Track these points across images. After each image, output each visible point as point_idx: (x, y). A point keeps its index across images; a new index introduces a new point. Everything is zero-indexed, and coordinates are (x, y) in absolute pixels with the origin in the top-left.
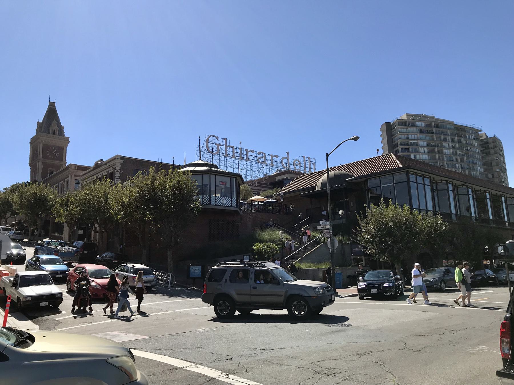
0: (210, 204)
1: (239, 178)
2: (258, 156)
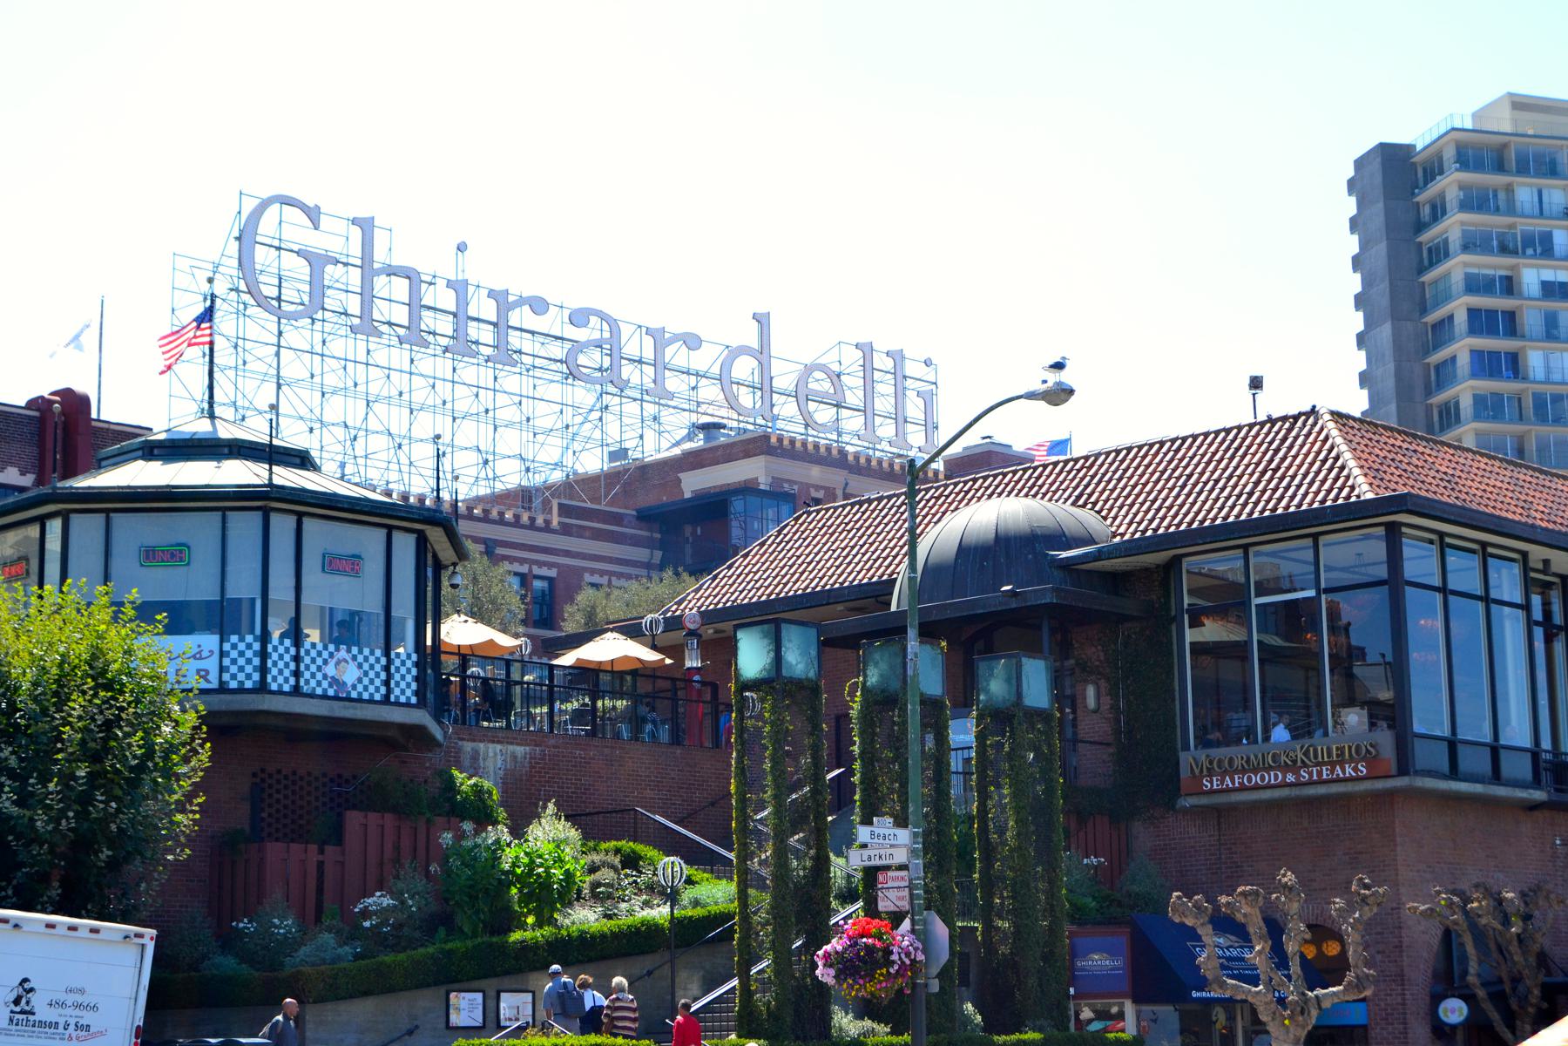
0: (262, 687)
1: (436, 535)
2: (572, 332)
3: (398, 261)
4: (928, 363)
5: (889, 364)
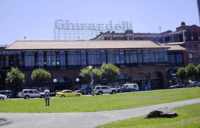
5: (126, 23)
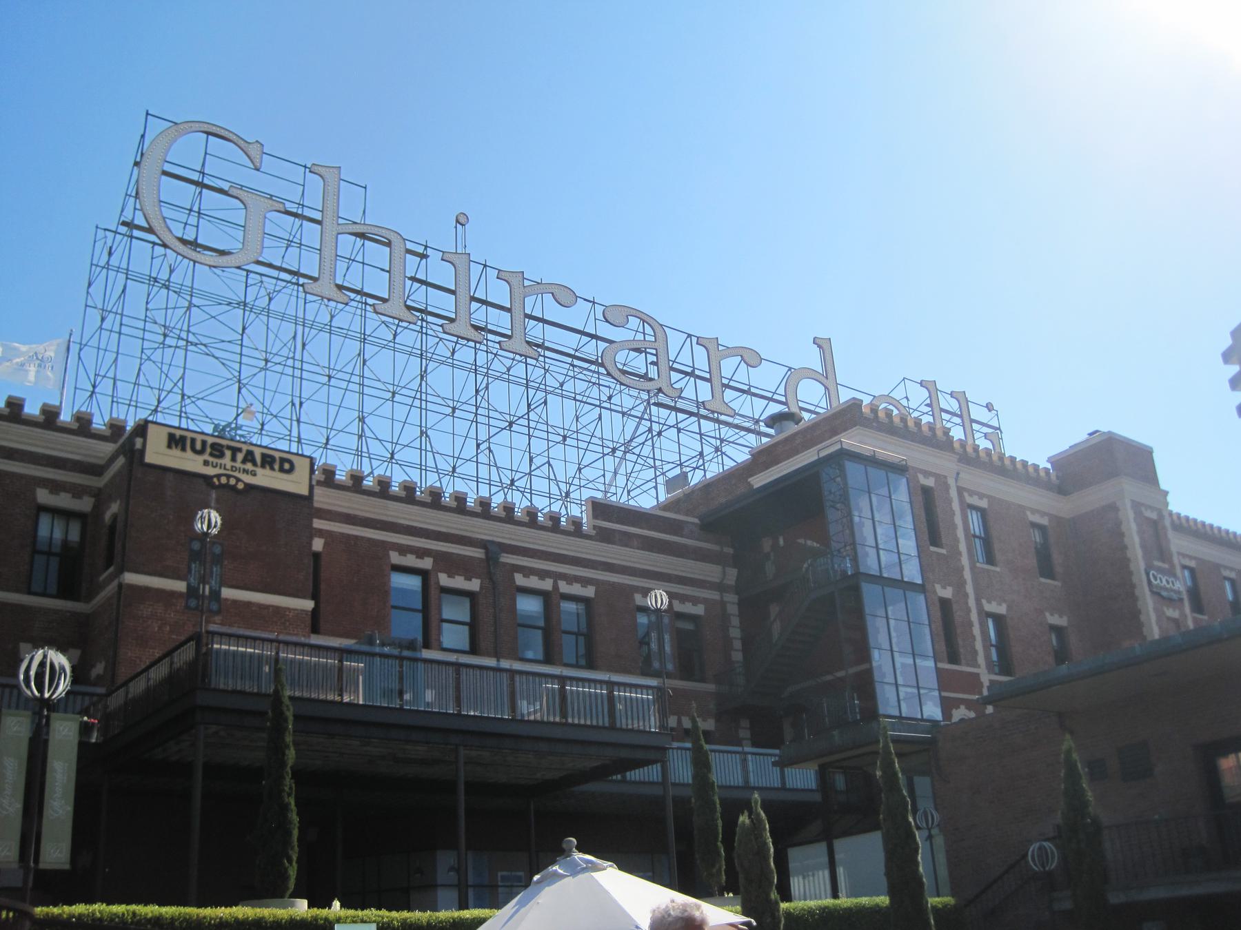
2: (605, 330)
3: (375, 220)
4: (989, 407)
5: (953, 405)
